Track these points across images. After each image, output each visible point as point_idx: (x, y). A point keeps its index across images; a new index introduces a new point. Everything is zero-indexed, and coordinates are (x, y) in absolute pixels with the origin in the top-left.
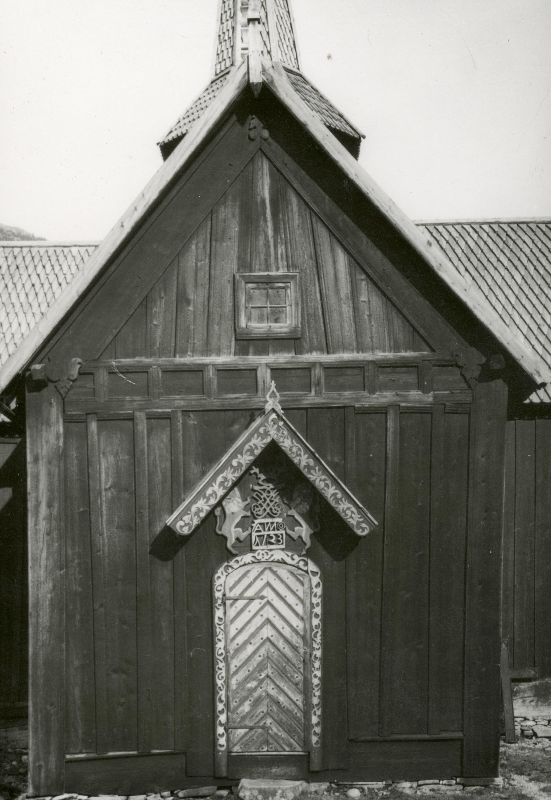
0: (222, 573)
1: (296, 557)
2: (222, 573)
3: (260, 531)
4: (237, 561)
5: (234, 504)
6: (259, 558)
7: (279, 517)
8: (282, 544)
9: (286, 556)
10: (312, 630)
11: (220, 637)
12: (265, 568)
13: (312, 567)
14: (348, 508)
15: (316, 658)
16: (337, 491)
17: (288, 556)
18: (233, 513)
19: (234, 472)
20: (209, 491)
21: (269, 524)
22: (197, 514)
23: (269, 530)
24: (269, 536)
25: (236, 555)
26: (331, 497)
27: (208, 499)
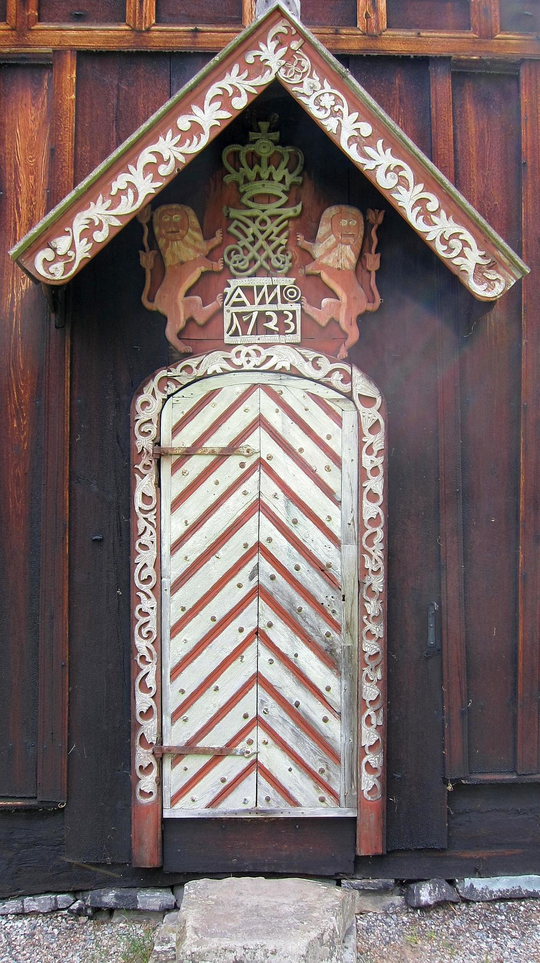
0: (153, 393)
1: (326, 364)
2: (153, 393)
3: (242, 304)
4: (187, 368)
5: (186, 244)
6: (237, 362)
7: (287, 275)
8: (294, 332)
9: (302, 359)
10: (361, 529)
11: (145, 539)
12: (254, 387)
13: (362, 385)
14: (455, 235)
15: (371, 593)
16: (425, 195)
17: (307, 360)
18: (182, 263)
19: (180, 143)
20: (120, 182)
21: (265, 289)
22: (86, 234)
23: (263, 302)
24: (263, 317)
25: (188, 355)
26: (413, 207)
27: (116, 201)
